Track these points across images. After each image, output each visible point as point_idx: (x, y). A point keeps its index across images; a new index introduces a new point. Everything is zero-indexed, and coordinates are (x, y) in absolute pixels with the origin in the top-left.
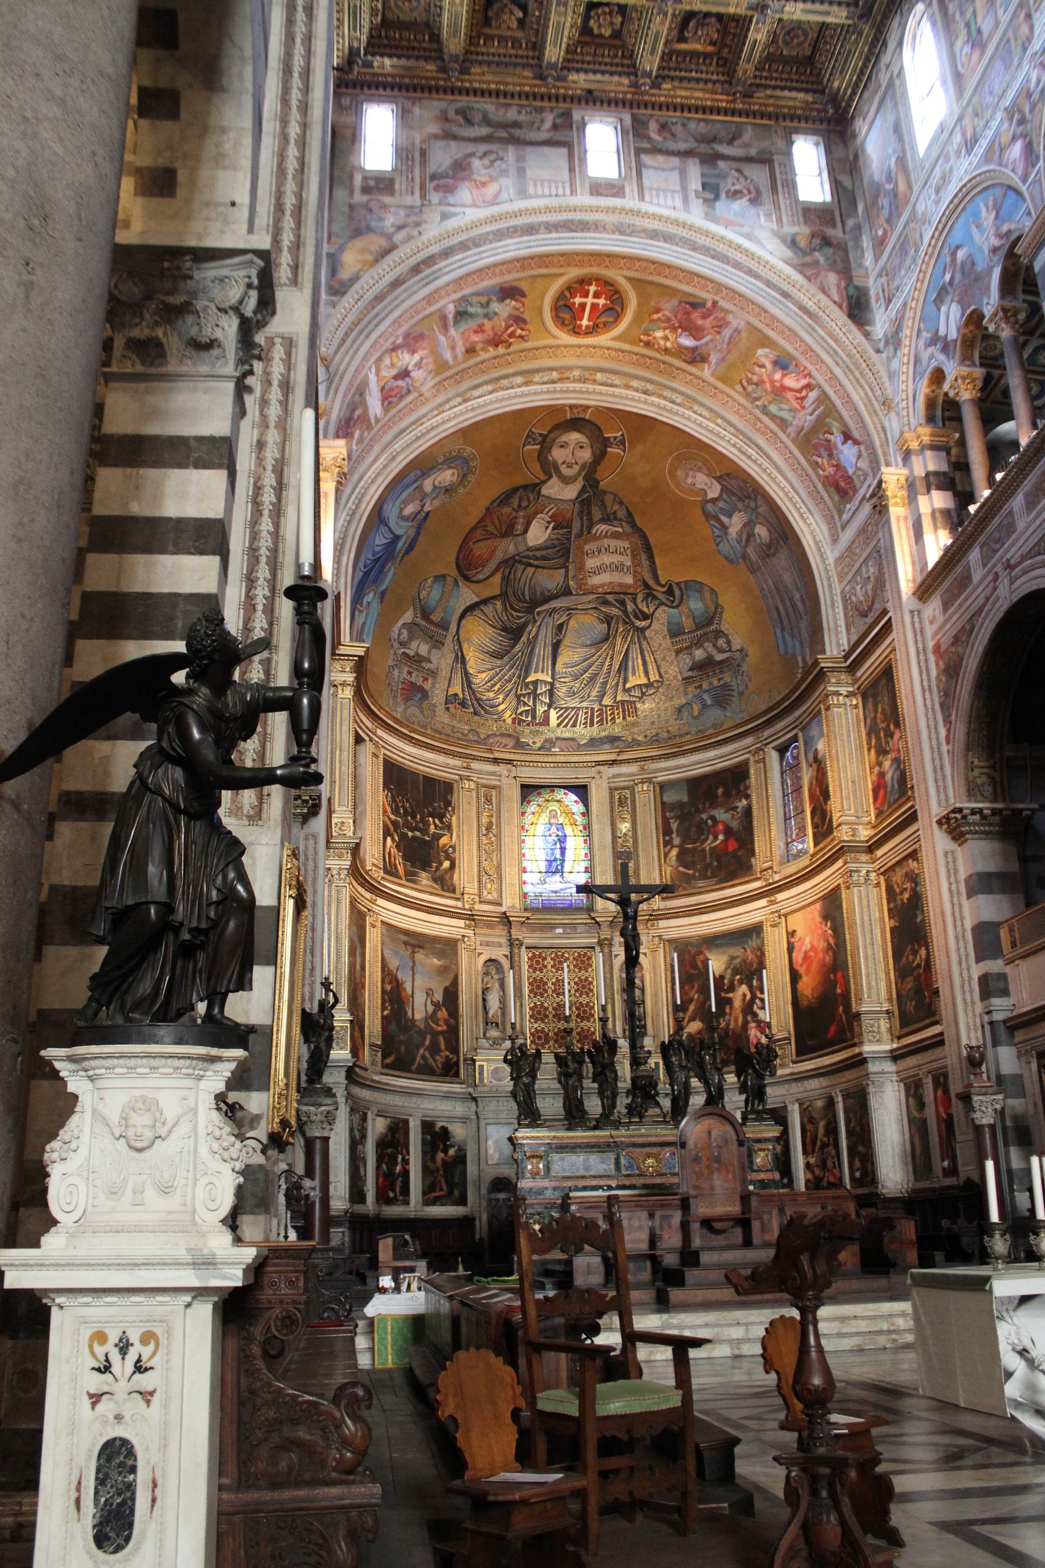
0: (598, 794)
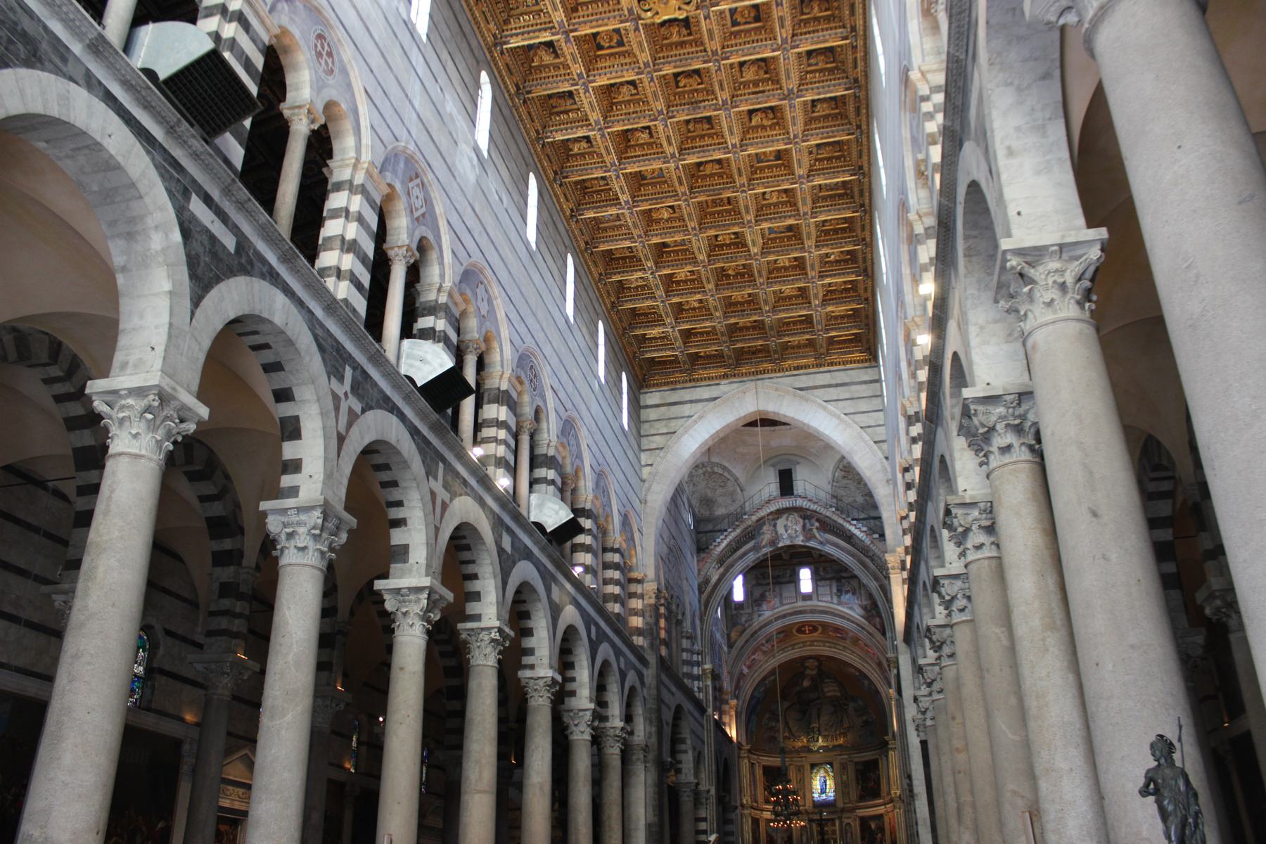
0: (836, 765)
